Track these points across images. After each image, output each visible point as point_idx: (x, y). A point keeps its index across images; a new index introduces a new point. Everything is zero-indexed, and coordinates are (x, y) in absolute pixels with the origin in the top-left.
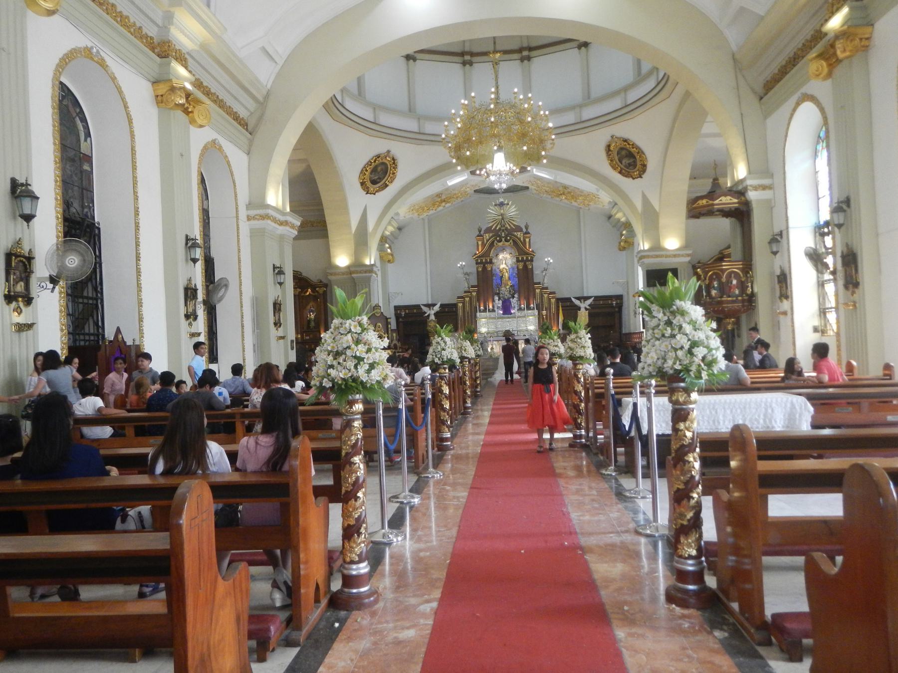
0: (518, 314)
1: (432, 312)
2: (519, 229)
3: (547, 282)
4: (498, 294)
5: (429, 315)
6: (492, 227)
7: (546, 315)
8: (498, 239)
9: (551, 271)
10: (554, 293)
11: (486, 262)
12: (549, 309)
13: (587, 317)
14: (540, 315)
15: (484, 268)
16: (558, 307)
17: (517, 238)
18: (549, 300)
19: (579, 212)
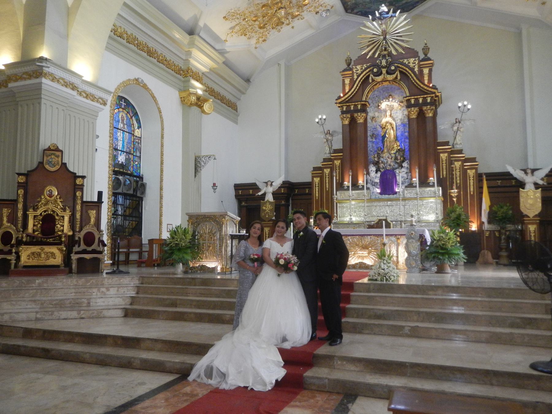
0: (409, 193)
1: (270, 190)
2: (412, 53)
3: (460, 142)
4: (376, 164)
5: (264, 194)
6: (367, 54)
7: (457, 197)
8: (375, 70)
9: (468, 123)
10: (473, 160)
11: (356, 111)
12: (463, 187)
13: (539, 200)
14: (446, 195)
15: (353, 121)
16: (481, 188)
17: (407, 66)
18: (464, 172)
19: (519, 34)
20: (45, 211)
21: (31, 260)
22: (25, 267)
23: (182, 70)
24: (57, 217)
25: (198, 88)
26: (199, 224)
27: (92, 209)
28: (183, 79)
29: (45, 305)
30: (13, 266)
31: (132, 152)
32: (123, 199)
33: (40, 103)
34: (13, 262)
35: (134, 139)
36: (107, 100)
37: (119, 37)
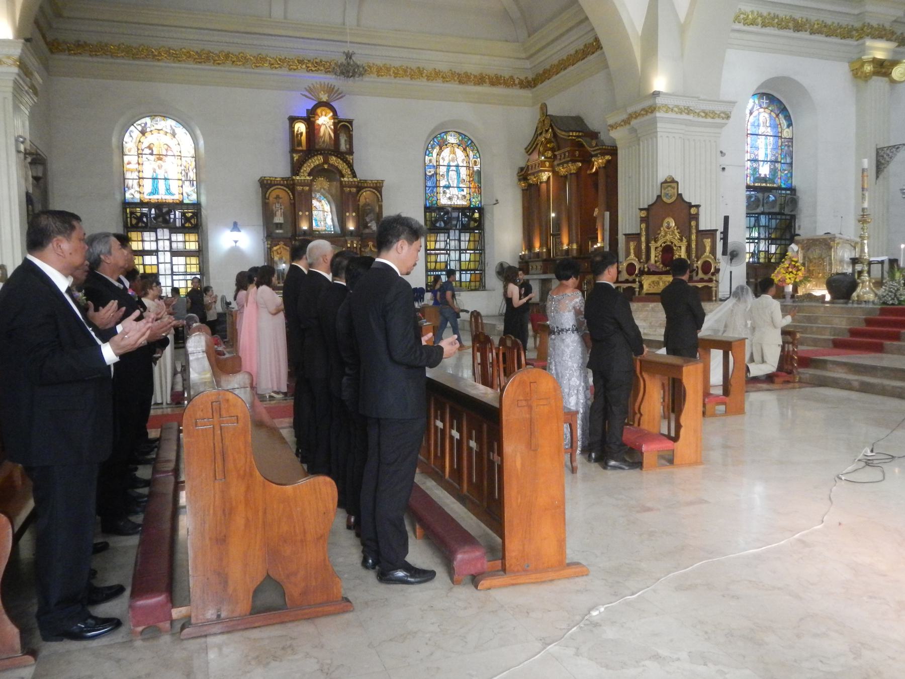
20: (664, 243)
21: (652, 288)
22: (647, 294)
23: (855, 30)
24: (675, 248)
25: (879, 50)
26: (809, 249)
27: (707, 238)
28: (856, 43)
29: (652, 324)
30: (637, 293)
31: (779, 160)
32: (767, 220)
33: (656, 137)
34: (637, 290)
35: (782, 142)
36: (730, 112)
37: (751, 26)
